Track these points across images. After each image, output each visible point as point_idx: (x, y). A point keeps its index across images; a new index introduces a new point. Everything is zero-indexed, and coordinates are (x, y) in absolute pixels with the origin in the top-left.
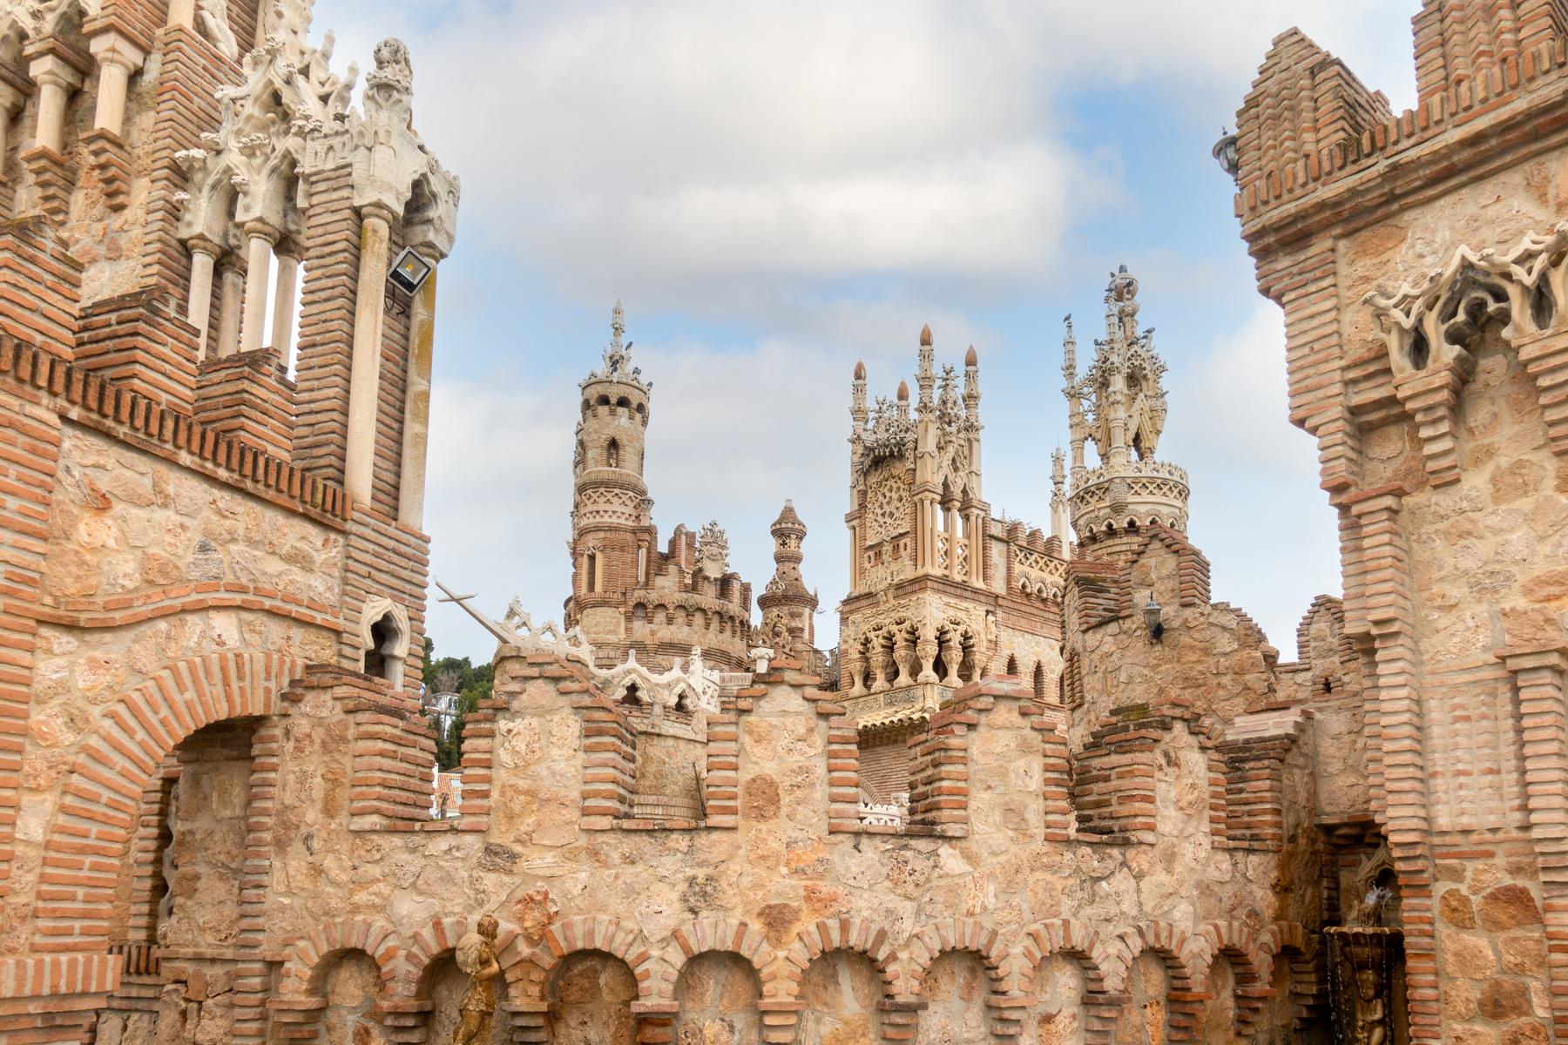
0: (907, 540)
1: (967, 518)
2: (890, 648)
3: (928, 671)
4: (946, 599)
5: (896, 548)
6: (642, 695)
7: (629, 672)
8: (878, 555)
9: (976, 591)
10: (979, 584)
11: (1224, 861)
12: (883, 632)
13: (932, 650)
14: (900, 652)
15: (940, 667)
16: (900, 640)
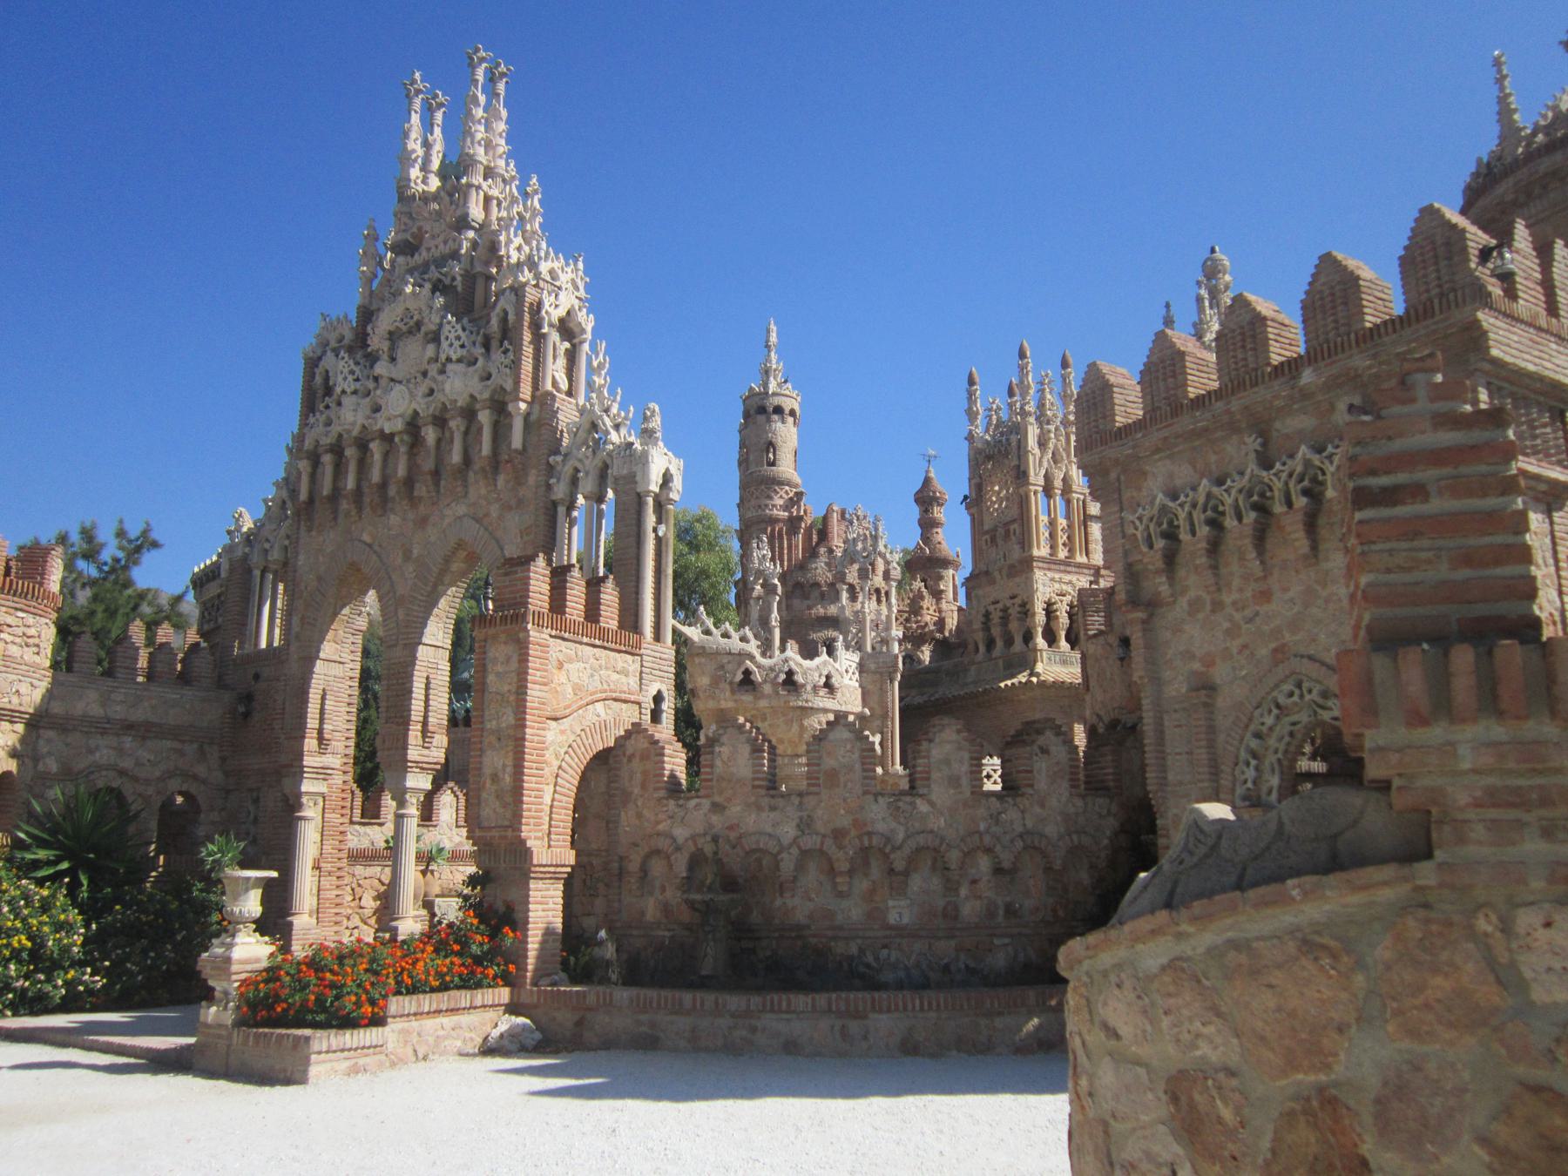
0: (1015, 526)
1: (1068, 502)
2: (1005, 619)
3: (1040, 642)
4: (1050, 574)
5: (1007, 533)
6: (799, 678)
7: (786, 661)
8: (993, 540)
9: (1080, 566)
10: (1081, 558)
11: (1079, 803)
12: (1000, 606)
13: (1040, 618)
14: (1014, 626)
15: (1051, 637)
16: (1013, 611)
